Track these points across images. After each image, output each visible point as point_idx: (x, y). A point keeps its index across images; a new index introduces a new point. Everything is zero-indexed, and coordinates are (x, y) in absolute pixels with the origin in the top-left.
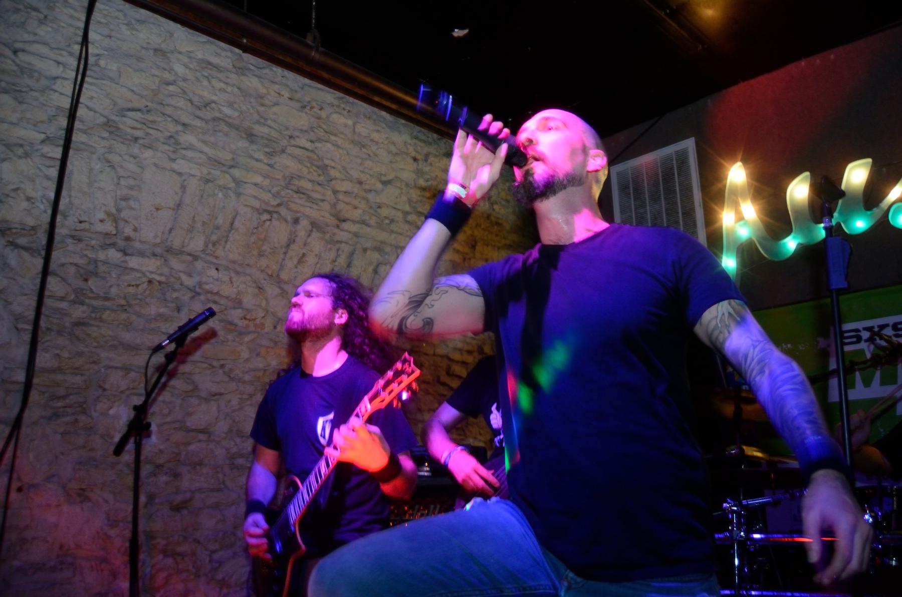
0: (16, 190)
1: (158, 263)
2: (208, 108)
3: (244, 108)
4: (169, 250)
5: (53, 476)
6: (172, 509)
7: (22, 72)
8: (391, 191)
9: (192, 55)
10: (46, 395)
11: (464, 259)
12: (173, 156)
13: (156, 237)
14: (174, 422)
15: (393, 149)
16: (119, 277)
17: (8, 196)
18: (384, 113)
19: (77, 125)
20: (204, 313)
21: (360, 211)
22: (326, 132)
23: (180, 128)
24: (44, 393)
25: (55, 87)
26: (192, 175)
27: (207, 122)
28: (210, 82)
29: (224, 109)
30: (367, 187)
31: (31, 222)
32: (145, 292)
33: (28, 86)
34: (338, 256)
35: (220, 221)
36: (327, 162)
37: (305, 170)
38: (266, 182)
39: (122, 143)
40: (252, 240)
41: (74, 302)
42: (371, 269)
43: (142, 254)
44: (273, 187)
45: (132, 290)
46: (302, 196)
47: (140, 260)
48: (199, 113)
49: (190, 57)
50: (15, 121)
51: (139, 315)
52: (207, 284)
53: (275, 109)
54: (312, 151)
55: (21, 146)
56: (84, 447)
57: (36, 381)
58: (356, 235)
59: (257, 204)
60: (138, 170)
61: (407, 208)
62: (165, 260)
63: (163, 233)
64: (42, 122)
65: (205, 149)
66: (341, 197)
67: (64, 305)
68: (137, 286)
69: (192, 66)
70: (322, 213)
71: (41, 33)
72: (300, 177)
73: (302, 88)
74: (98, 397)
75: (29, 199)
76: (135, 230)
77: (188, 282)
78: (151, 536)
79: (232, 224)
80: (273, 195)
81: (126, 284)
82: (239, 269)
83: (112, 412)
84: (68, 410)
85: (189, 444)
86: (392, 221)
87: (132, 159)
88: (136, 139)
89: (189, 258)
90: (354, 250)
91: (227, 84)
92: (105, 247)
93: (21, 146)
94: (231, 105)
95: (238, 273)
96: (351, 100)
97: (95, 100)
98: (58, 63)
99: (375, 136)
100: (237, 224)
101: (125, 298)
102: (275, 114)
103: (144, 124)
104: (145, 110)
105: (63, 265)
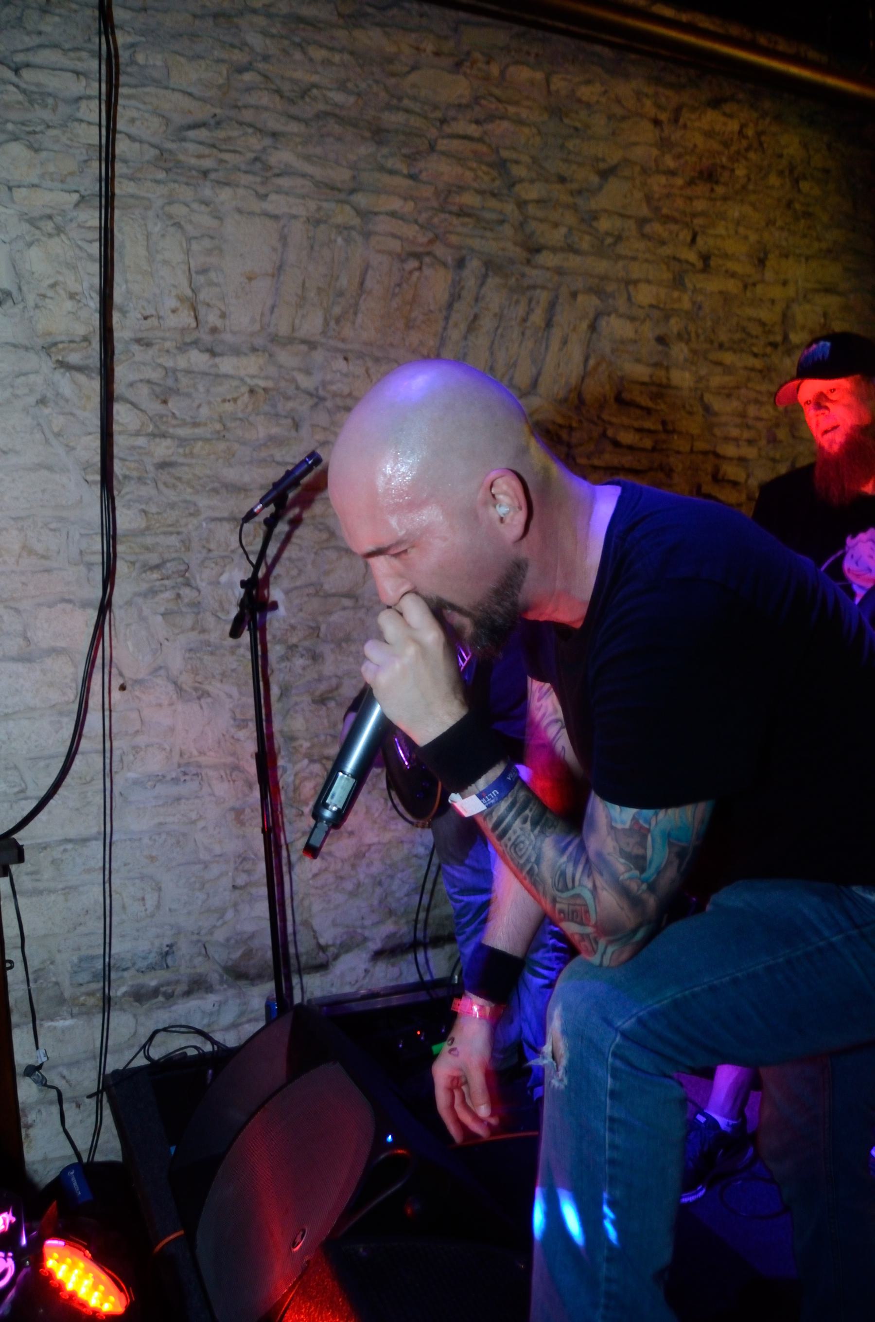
0: (53, 286)
1: (261, 361)
2: (307, 99)
3: (363, 86)
4: (274, 339)
5: (161, 668)
6: (314, 702)
7: (31, 102)
8: (614, 186)
9: (273, 10)
10: (137, 565)
11: (745, 287)
12: (262, 190)
13: (253, 320)
14: (308, 586)
15: (619, 111)
16: (208, 391)
17: (44, 296)
18: (598, 48)
19: (119, 168)
20: (304, 461)
21: (563, 230)
22: (499, 100)
23: (268, 141)
24: (133, 563)
25: (80, 115)
26: (295, 217)
27: (306, 122)
28: (305, 53)
29: (331, 95)
30: (575, 186)
31: (81, 330)
32: (247, 407)
33: (43, 121)
34: (530, 311)
35: (344, 282)
36: (505, 154)
37: (469, 175)
38: (409, 206)
39: (187, 184)
40: (394, 304)
41: (153, 435)
42: (584, 325)
43: (236, 352)
44: (420, 212)
45: (229, 407)
46: (466, 220)
47: (234, 360)
48: (293, 110)
49: (269, 16)
50: (36, 181)
51: (243, 443)
52: (332, 383)
53: (414, 77)
54: (480, 140)
55: (50, 217)
56: (193, 629)
57: (120, 548)
58: (559, 271)
59: (395, 245)
60: (215, 223)
61: (645, 211)
62: (270, 355)
63: (262, 314)
64: (71, 174)
65: (309, 169)
67: (141, 441)
68: (235, 400)
69: (274, 31)
71: (47, 29)
72: (462, 189)
73: (456, 30)
74: (203, 562)
75: (72, 296)
76: (223, 316)
77: (304, 382)
78: (291, 738)
79: (362, 283)
80: (422, 227)
81: (219, 400)
82: (378, 354)
83: (224, 579)
84: (166, 582)
85: (330, 613)
86: (619, 238)
87: (203, 207)
88: (205, 173)
89: (304, 348)
90: (557, 297)
91: (331, 49)
92: (183, 348)
93: (50, 217)
94: (342, 86)
95: (377, 360)
96: (540, 34)
97: (138, 123)
98: (77, 73)
99: (586, 92)
100: (369, 284)
101: (221, 420)
102: (414, 86)
103: (214, 146)
104: (212, 122)
105: (131, 385)
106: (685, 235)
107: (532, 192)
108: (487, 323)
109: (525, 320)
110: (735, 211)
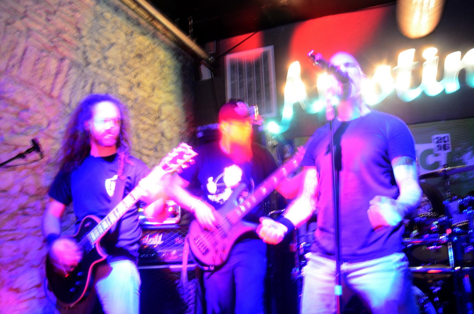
58: (96, 73)
66: (88, 48)
70: (78, 57)
106: (133, 74)
107: (88, 42)
108: (70, 85)
109: (84, 87)
110: (147, 70)
